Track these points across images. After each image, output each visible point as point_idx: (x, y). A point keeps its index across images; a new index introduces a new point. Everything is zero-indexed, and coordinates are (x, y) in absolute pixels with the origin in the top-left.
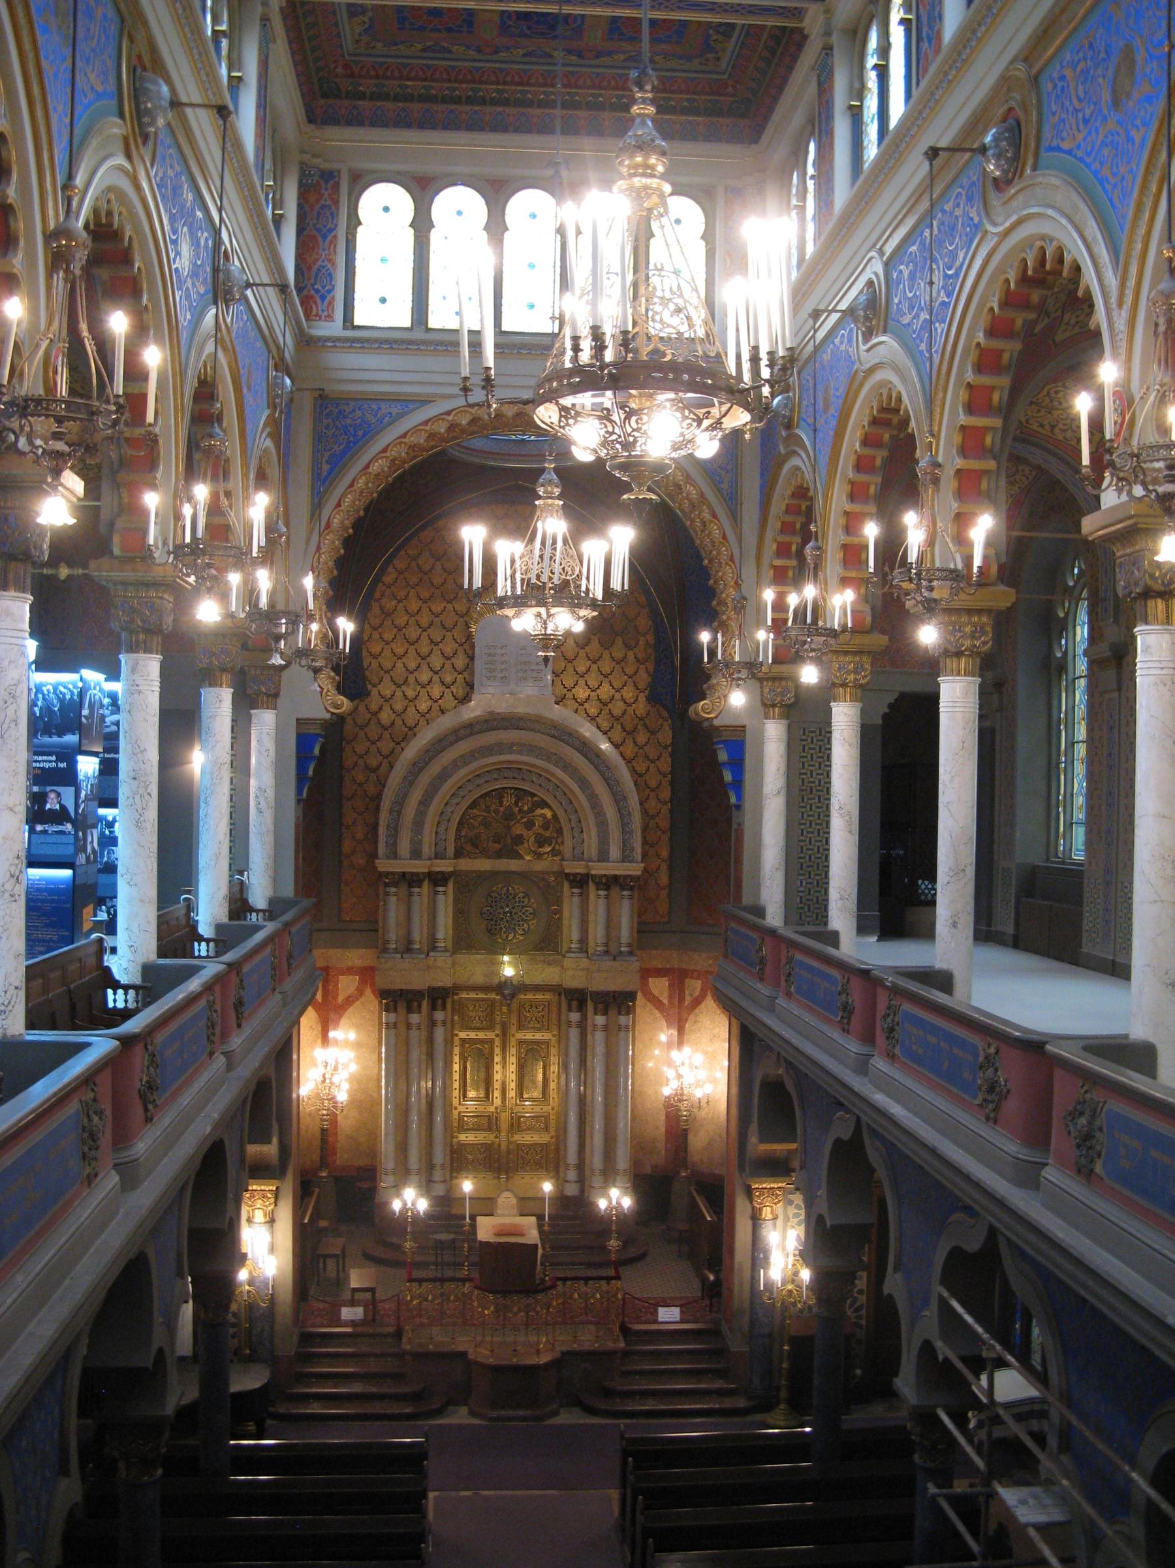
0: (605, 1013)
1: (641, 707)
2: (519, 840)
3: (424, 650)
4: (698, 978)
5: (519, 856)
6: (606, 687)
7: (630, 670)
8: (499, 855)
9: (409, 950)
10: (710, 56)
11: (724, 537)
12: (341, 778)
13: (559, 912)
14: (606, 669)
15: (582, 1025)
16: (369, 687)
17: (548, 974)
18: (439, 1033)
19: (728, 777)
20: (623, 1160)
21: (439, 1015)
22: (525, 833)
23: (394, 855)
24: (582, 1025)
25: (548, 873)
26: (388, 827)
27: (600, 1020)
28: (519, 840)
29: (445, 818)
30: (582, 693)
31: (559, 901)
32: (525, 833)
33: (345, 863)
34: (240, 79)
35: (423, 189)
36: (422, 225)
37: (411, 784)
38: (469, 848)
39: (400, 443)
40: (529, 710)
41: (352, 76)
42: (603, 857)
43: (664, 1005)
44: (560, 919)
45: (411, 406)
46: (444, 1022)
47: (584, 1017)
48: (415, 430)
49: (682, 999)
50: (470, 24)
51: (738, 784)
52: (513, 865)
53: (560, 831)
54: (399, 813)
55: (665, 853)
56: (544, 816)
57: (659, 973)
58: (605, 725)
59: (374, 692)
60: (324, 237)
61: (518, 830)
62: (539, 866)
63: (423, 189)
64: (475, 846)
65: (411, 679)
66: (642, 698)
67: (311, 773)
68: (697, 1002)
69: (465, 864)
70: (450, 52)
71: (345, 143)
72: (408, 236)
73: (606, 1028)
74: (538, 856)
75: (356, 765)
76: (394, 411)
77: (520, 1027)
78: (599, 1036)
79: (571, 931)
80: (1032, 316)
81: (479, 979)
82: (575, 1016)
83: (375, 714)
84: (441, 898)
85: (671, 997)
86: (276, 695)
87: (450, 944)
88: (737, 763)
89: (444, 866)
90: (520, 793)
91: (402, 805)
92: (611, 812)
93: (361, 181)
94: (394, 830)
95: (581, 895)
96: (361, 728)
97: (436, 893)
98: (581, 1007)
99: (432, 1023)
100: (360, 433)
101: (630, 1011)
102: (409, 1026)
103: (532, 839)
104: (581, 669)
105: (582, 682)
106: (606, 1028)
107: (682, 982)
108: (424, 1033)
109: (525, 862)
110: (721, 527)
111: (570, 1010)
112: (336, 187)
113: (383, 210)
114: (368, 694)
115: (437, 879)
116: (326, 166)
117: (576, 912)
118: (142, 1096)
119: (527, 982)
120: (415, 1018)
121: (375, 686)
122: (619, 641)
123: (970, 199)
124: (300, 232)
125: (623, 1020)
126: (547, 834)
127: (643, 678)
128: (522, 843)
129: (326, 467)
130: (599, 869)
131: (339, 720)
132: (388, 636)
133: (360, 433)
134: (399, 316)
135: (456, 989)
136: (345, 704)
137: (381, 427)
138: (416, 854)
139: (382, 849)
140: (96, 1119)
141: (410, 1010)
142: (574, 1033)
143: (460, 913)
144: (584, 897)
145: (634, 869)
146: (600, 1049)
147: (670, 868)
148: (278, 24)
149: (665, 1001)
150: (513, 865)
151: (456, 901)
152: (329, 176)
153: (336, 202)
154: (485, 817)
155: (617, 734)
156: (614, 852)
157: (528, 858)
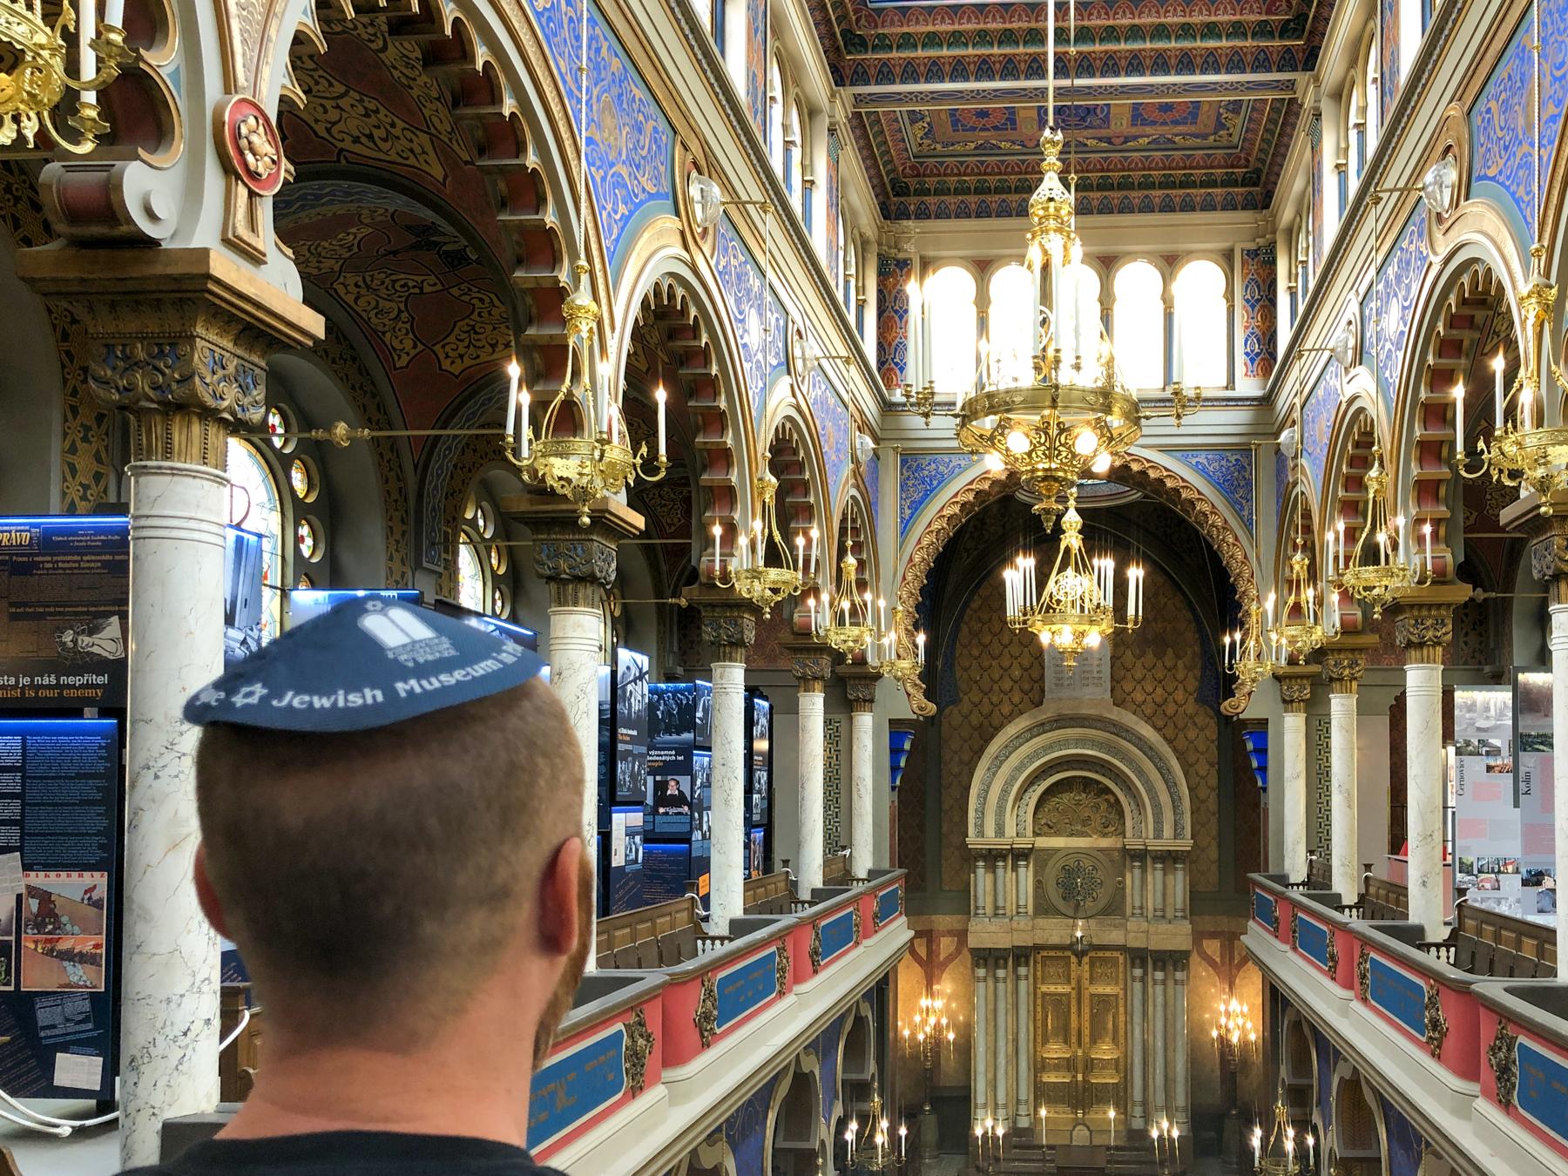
0: (1163, 969)
1: (1191, 707)
3: (1006, 664)
6: (1159, 691)
7: (1180, 676)
9: (996, 915)
13: (1122, 883)
14: (1160, 675)
15: (1143, 980)
17: (1115, 937)
18: (1023, 985)
19: (1255, 764)
20: (1181, 1100)
21: (1022, 971)
23: (981, 833)
24: (1143, 980)
27: (1159, 975)
30: (1139, 697)
34: (812, 182)
40: (1092, 712)
41: (918, 175)
42: (1158, 834)
44: (1124, 889)
47: (1145, 973)
49: (1232, 959)
51: (1263, 769)
53: (1121, 814)
55: (1214, 832)
56: (1107, 801)
58: (1160, 723)
65: (996, 687)
66: (1191, 699)
67: (902, 764)
69: (1042, 842)
74: (1105, 835)
77: (1092, 980)
78: (1159, 989)
79: (1132, 897)
80: (1477, 335)
81: (1055, 939)
82: (1138, 972)
84: (1022, 870)
85: (1222, 956)
86: (872, 701)
87: (1030, 909)
88: (1262, 752)
89: (1023, 843)
90: (1087, 783)
92: (1164, 798)
94: (981, 813)
98: (1143, 966)
101: (1185, 967)
104: (1138, 675)
105: (1139, 688)
106: (1164, 982)
108: (1010, 986)
111: (1133, 966)
117: (1137, 882)
118: (699, 1026)
119: (1095, 941)
120: (1001, 973)
122: (1170, 652)
123: (1420, 235)
124: (880, 315)
125: (1179, 975)
127: (1192, 684)
129: (908, 512)
130: (1155, 845)
131: (931, 720)
132: (976, 652)
135: (1037, 948)
136: (932, 708)
138: (1000, 831)
139: (971, 830)
140: (641, 1042)
141: (997, 966)
142: (1138, 986)
144: (1144, 869)
145: (1186, 844)
146: (1160, 1000)
147: (1219, 846)
148: (845, 133)
151: (1036, 874)
155: (1169, 732)
156: (1168, 831)
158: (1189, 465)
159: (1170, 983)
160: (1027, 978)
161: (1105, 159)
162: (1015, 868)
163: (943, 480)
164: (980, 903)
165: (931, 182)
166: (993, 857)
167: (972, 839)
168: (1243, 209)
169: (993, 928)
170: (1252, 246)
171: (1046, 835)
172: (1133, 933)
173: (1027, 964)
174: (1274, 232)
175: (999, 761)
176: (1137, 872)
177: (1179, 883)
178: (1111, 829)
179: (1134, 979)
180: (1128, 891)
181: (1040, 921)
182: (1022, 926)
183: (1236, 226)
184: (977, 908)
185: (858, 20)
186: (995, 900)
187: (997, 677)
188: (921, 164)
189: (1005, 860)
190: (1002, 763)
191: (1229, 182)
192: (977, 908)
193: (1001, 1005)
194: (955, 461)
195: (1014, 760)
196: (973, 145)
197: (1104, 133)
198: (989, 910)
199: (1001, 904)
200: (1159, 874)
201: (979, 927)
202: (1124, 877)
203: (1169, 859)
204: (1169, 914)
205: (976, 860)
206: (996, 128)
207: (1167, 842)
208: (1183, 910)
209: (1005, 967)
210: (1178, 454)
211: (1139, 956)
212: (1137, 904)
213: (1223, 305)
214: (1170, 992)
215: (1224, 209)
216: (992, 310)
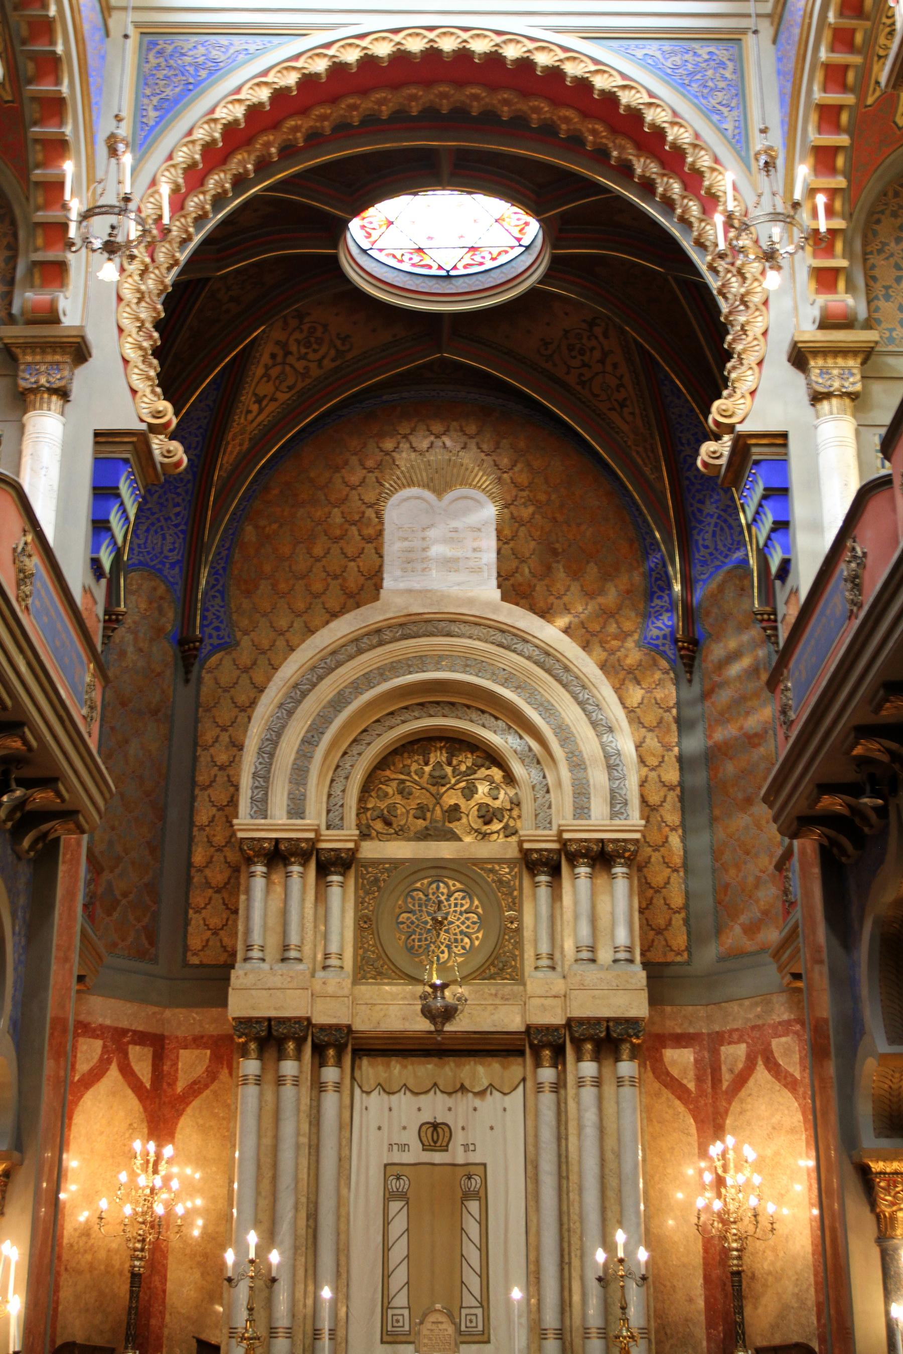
2: (454, 812)
3: (318, 587)
4: (740, 1040)
5: (454, 837)
8: (424, 836)
12: (195, 759)
13: (519, 919)
15: (559, 1086)
16: (239, 634)
18: (330, 1100)
22: (462, 802)
23: (261, 807)
25: (500, 861)
26: (255, 775)
27: (589, 1068)
28: (454, 812)
29: (342, 773)
31: (516, 904)
32: (462, 802)
33: (197, 879)
37: (290, 713)
38: (379, 825)
43: (688, 1091)
44: (519, 931)
46: (338, 1087)
49: (716, 1080)
52: (444, 850)
54: (272, 755)
57: (681, 1040)
59: (245, 642)
61: (451, 798)
62: (484, 850)
64: (388, 824)
68: (742, 1080)
69: (370, 850)
73: (598, 1082)
74: (485, 836)
75: (216, 740)
78: (588, 1094)
82: (547, 1074)
83: (246, 670)
84: (335, 892)
91: (275, 743)
94: (263, 777)
95: (550, 885)
96: (226, 690)
97: (328, 885)
99: (319, 1087)
102: (279, 1081)
103: (474, 812)
106: (598, 1082)
107: (715, 1052)
109: (468, 846)
111: (538, 1064)
114: (238, 644)
115: (331, 865)
120: (289, 1067)
121: (246, 633)
126: (497, 804)
128: (459, 819)
138: (297, 810)
142: (547, 1099)
143: (365, 924)
146: (590, 1117)
149: (691, 1086)
150: (444, 850)
151: (359, 903)
154: (403, 782)
156: (599, 810)
157: (468, 839)
159: (609, 1089)
160: (338, 1087)
162: (321, 897)
164: (256, 938)
166: (278, 855)
167: (246, 823)
169: (277, 981)
171: (380, 836)
172: (543, 999)
173: (339, 1063)
175: (299, 691)
176: (543, 892)
177: (618, 896)
178: (496, 826)
179: (539, 1088)
180: (528, 934)
181: (366, 991)
182: (331, 989)
184: (249, 948)
186: (285, 933)
187: (300, 605)
189: (304, 864)
190: (304, 695)
192: (249, 948)
193: (288, 1128)
195: (327, 689)
198: (272, 952)
199: (294, 940)
200: (583, 883)
201: (250, 980)
202: (520, 911)
203: (601, 857)
204: (605, 955)
205: (249, 861)
207: (600, 822)
208: (630, 949)
209: (298, 1057)
211: (545, 1045)
212: (544, 948)
214: (610, 1108)
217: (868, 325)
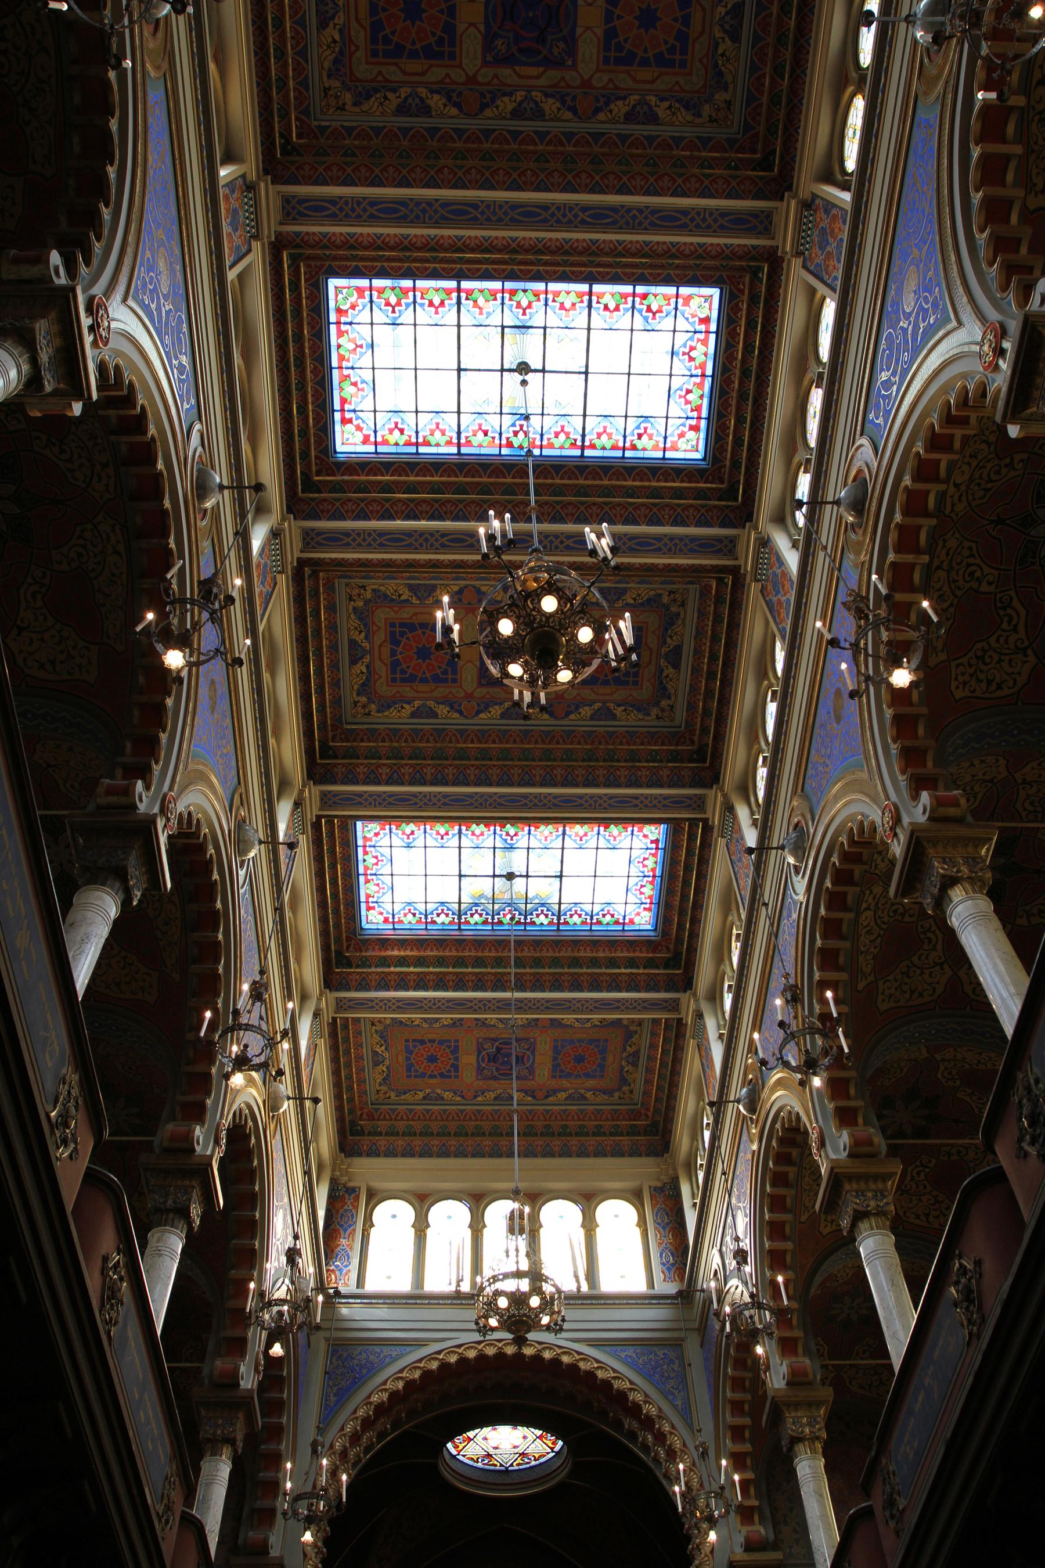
10: (625, 1088)
11: (684, 1445)
35: (422, 1202)
36: (421, 1226)
39: (398, 1378)
45: (408, 1349)
48: (412, 1367)
50: (457, 1070)
60: (345, 1230)
63: (422, 1202)
70: (442, 1099)
71: (366, 1170)
72: (409, 1235)
76: (394, 1354)
93: (375, 1197)
100: (365, 1371)
110: (681, 1438)
112: (357, 1198)
113: (393, 1219)
116: (351, 1184)
129: (333, 1399)
133: (365, 1371)
134: (403, 1284)
137: (383, 1366)
152: (353, 1191)
153: (357, 1208)
158: (619, 1358)
161: (530, 1111)
163: (372, 1369)
165: (383, 1125)
168: (647, 1155)
170: (659, 1184)
174: (675, 1169)
183: (644, 1170)
185: (348, 947)
188: (377, 1110)
191: (633, 1131)
194: (386, 1351)
196: (421, 1095)
197: (531, 1084)
206: (442, 1075)
210: (608, 1349)
213: (637, 1232)
215: (630, 1155)
216: (429, 1231)
217: (775, 1546)
